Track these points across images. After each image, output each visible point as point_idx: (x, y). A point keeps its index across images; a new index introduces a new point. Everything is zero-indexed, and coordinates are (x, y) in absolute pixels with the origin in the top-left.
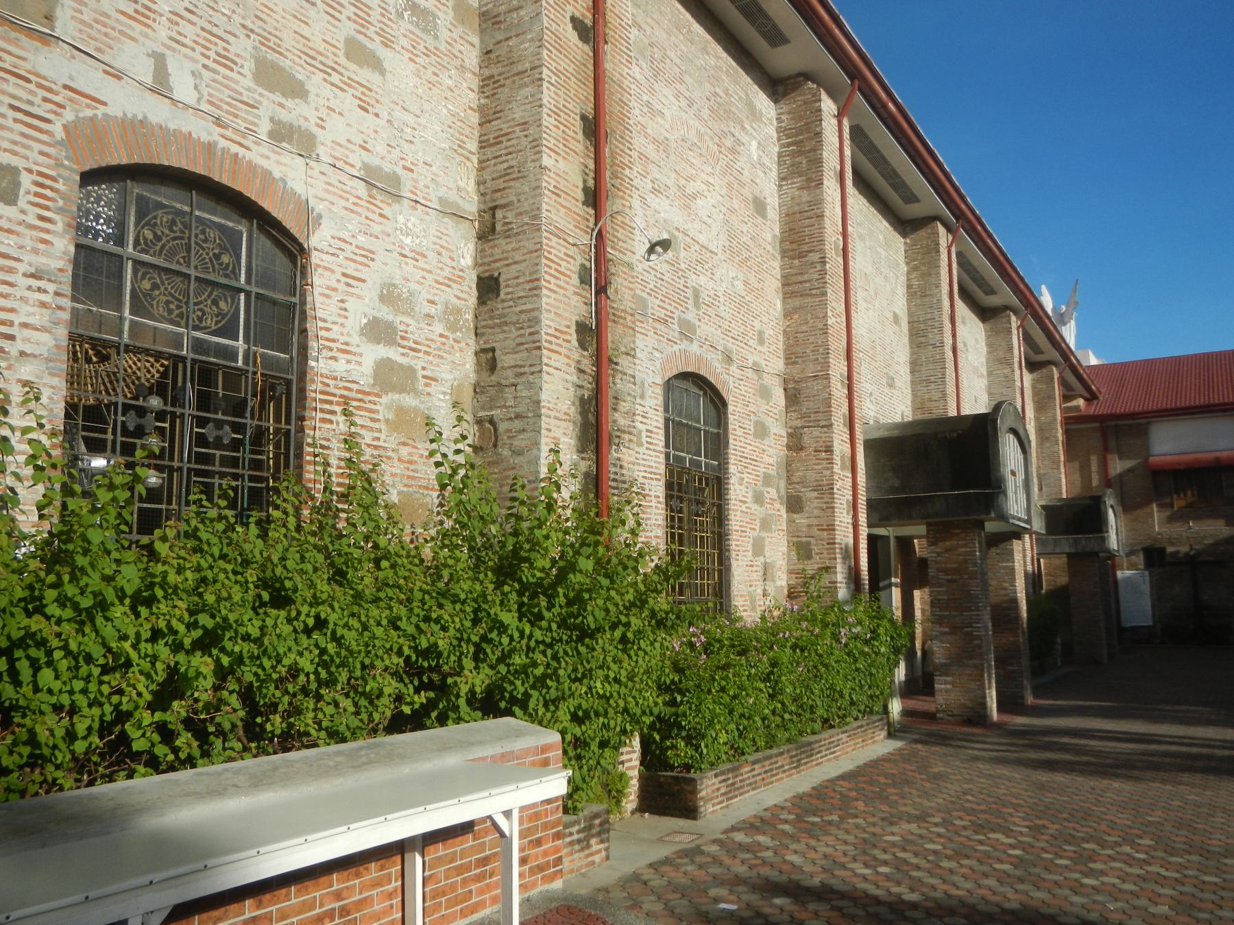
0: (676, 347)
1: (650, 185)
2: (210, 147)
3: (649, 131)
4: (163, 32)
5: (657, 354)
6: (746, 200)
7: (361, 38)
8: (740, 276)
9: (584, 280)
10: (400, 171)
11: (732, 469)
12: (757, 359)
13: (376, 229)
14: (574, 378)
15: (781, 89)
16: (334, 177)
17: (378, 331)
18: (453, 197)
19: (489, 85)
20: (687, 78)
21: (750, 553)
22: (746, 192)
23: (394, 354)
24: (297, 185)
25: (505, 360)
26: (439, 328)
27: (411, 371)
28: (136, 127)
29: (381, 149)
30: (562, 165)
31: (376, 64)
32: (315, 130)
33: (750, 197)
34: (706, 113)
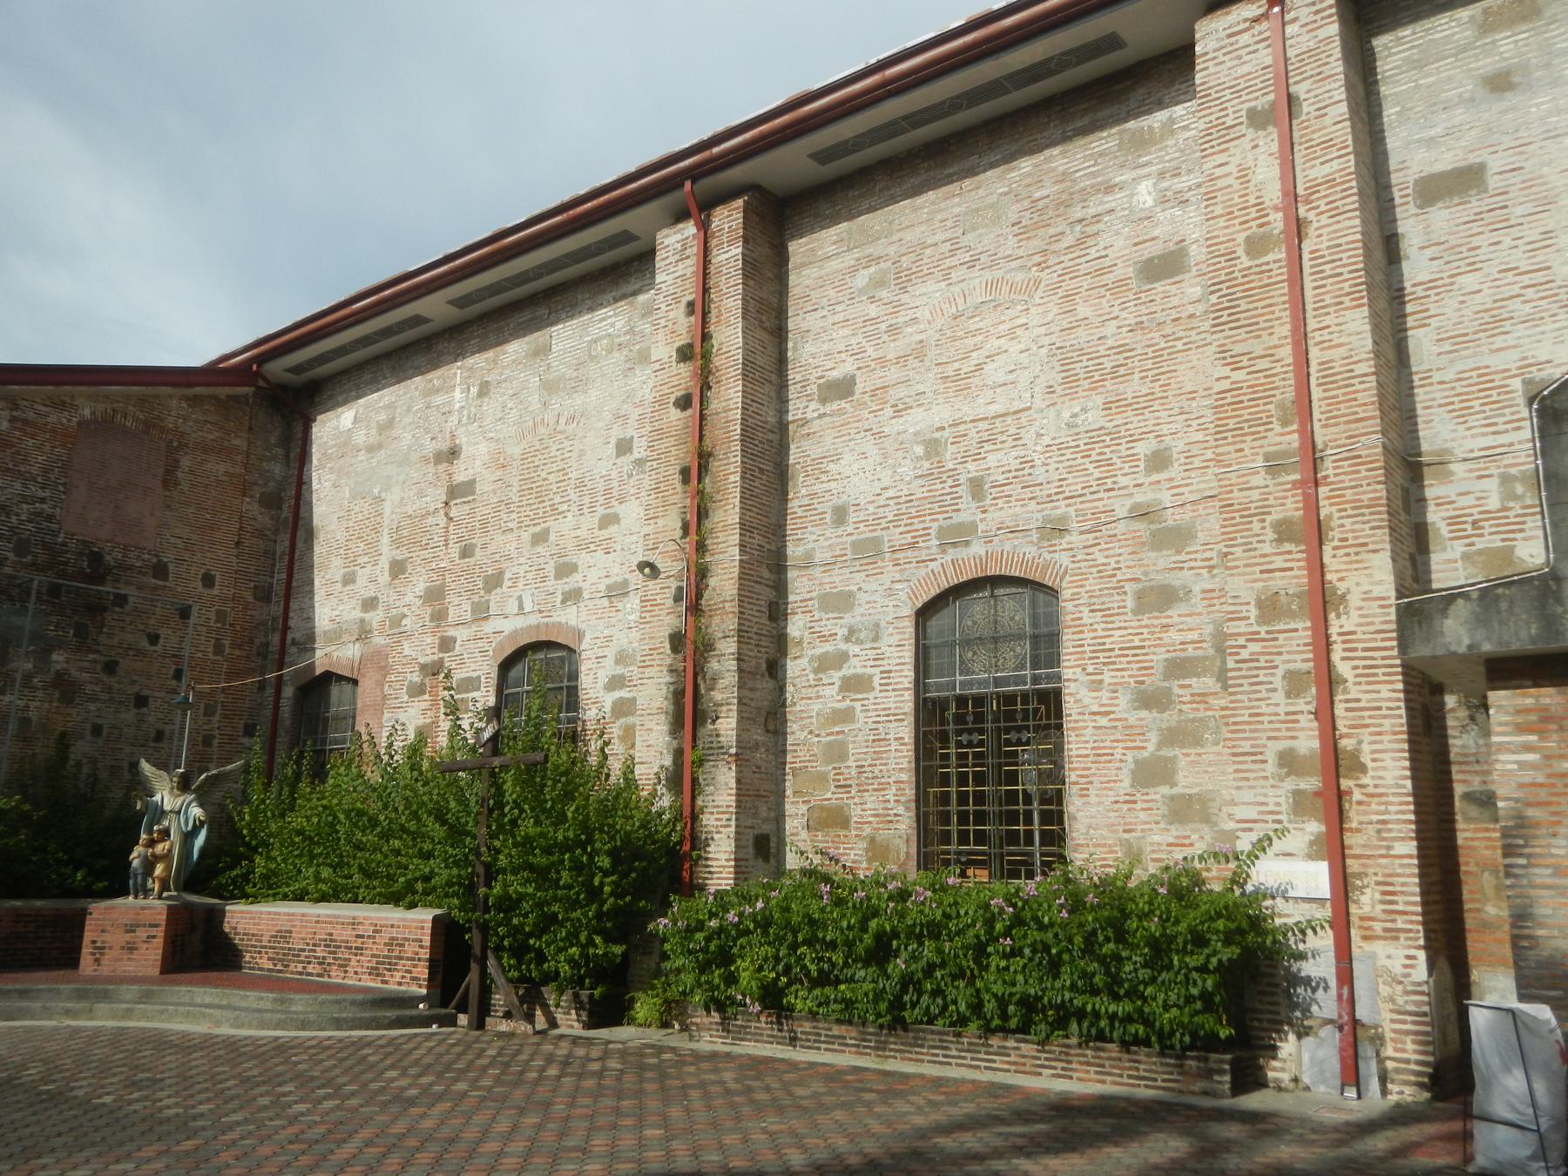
0: (932, 565)
1: (889, 411)
2: (538, 626)
4: (520, 585)
5: (898, 586)
7: (608, 511)
9: (677, 599)
10: (626, 576)
11: (1067, 673)
12: (1139, 498)
13: (613, 621)
14: (668, 679)
16: (591, 604)
17: (615, 683)
20: (964, 241)
21: (1127, 783)
22: (1125, 271)
23: (624, 693)
28: (515, 634)
30: (661, 522)
32: (581, 584)
33: (1130, 272)
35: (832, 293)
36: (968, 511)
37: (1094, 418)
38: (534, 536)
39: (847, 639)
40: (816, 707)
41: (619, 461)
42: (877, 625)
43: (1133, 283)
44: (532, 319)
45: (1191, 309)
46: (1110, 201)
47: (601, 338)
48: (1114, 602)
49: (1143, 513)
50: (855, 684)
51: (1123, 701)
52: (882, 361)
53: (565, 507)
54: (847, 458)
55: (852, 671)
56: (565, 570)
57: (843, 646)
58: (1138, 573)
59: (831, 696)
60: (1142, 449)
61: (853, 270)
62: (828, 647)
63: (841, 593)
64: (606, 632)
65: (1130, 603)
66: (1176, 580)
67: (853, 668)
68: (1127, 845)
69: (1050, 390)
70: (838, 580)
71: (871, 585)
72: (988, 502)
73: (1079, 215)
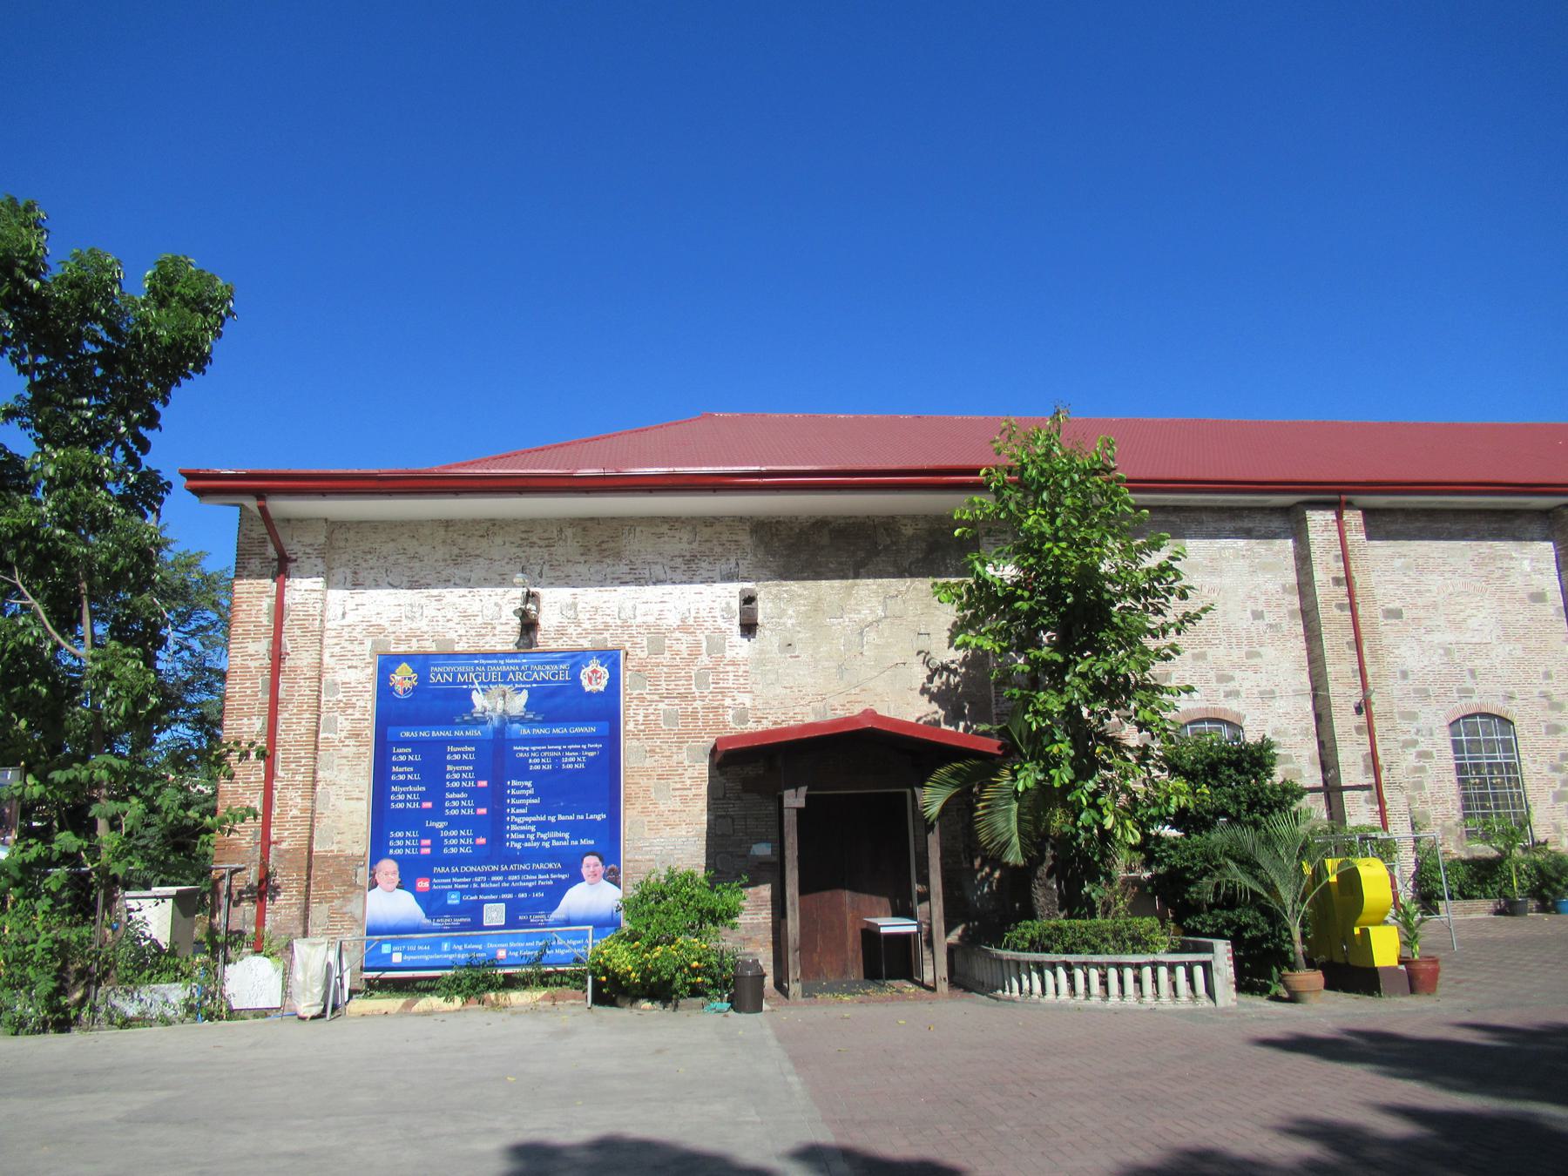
1: (1423, 631)
2: (1207, 709)
3: (1420, 604)
6: (1521, 601)
8: (1519, 646)
10: (1273, 688)
12: (1544, 689)
13: (1267, 711)
15: (1551, 515)
16: (1248, 701)
18: (1299, 687)
19: (1308, 639)
20: (1451, 560)
21: (1551, 800)
24: (1235, 709)
25: (1328, 745)
26: (1300, 737)
27: (1290, 756)
29: (1265, 683)
30: (1338, 667)
31: (1258, 655)
33: (1525, 596)
34: (1471, 569)
35: (1382, 565)
36: (1469, 684)
37: (1519, 653)
38: (1193, 655)
39: (1417, 734)
40: (1404, 765)
41: (1256, 622)
42: (1431, 729)
43: (1527, 601)
44: (1165, 521)
45: (1550, 618)
46: (1513, 564)
47: (1227, 548)
48: (1537, 729)
49: (1545, 695)
50: (1423, 755)
51: (1546, 769)
52: (1415, 605)
53: (1217, 642)
54: (1403, 648)
55: (1421, 749)
56: (1223, 678)
57: (1415, 737)
58: (1545, 718)
59: (1410, 759)
60: (1541, 669)
61: (1392, 557)
62: (1407, 737)
63: (1409, 712)
64: (1262, 717)
65: (1543, 730)
66: (1561, 723)
67: (1422, 747)
68: (1553, 824)
69: (1498, 637)
70: (1409, 706)
71: (1427, 710)
72: (1478, 680)
73: (1500, 565)
